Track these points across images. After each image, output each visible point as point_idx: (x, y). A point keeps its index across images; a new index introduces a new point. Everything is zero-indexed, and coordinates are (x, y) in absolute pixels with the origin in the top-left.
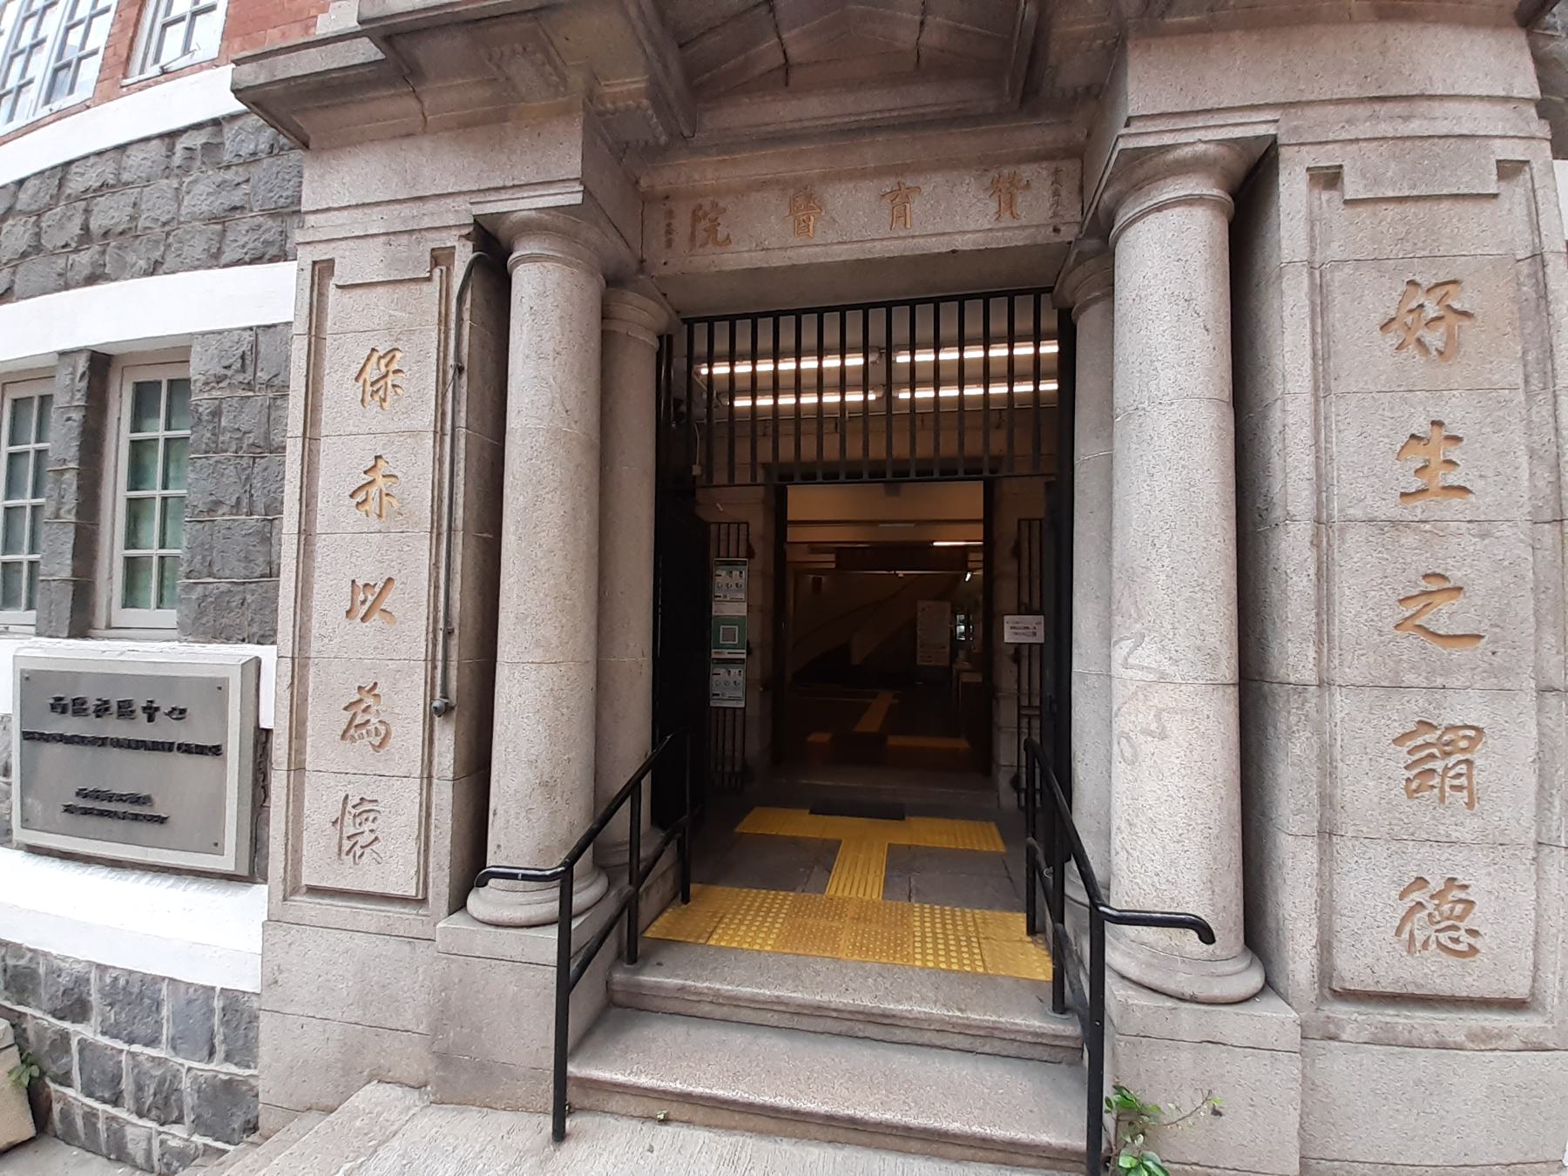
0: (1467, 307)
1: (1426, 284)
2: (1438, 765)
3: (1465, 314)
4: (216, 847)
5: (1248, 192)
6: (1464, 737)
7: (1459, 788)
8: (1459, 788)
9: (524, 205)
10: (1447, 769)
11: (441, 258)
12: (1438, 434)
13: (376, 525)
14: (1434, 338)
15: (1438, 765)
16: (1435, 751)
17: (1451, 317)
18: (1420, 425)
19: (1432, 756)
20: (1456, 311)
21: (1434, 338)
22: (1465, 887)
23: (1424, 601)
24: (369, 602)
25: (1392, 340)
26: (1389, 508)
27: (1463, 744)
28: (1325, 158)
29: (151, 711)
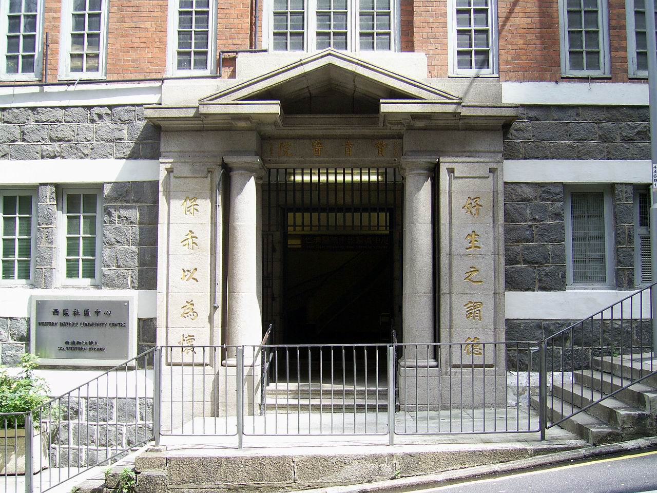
0: (481, 204)
1: (472, 198)
2: (472, 311)
3: (480, 206)
5: (434, 173)
6: (478, 305)
7: (477, 316)
8: (477, 316)
10: (475, 312)
12: (474, 234)
13: (188, 251)
14: (473, 210)
15: (472, 311)
16: (472, 308)
17: (477, 206)
18: (470, 233)
19: (472, 309)
20: (478, 205)
21: (473, 210)
22: (479, 339)
23: (470, 273)
24: (190, 274)
25: (464, 211)
26: (463, 251)
27: (478, 306)
28: (450, 166)
29: (97, 313)
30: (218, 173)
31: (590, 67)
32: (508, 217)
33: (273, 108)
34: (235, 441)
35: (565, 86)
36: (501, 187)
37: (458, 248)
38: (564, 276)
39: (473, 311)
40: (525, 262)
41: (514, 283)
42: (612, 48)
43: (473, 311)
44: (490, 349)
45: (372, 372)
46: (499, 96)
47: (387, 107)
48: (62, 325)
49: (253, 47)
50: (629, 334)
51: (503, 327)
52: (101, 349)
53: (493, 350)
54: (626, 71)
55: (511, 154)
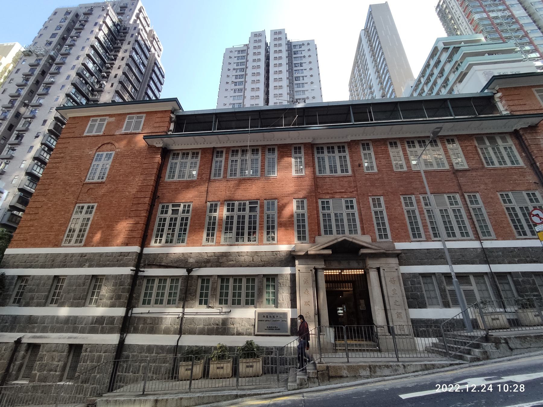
4: (287, 332)
9: (320, 267)
11: (311, 270)
30: (314, 271)
31: (419, 237)
32: (404, 285)
33: (329, 252)
34: (346, 360)
35: (412, 243)
36: (400, 275)
37: (390, 294)
38: (426, 303)
39: (399, 315)
40: (412, 298)
41: (410, 306)
42: (425, 232)
43: (399, 315)
44: (405, 328)
45: (366, 338)
46: (394, 247)
47: (363, 251)
48: (266, 321)
49: (319, 235)
50: (453, 324)
51: (410, 321)
52: (279, 329)
53: (408, 329)
54: (431, 238)
55: (401, 264)
